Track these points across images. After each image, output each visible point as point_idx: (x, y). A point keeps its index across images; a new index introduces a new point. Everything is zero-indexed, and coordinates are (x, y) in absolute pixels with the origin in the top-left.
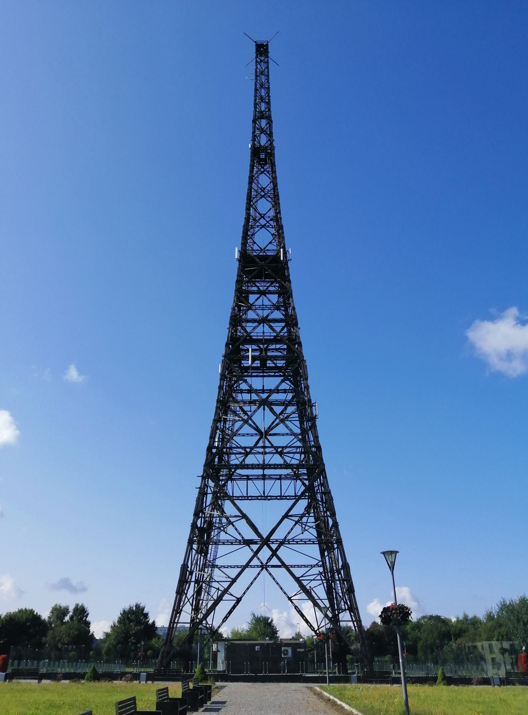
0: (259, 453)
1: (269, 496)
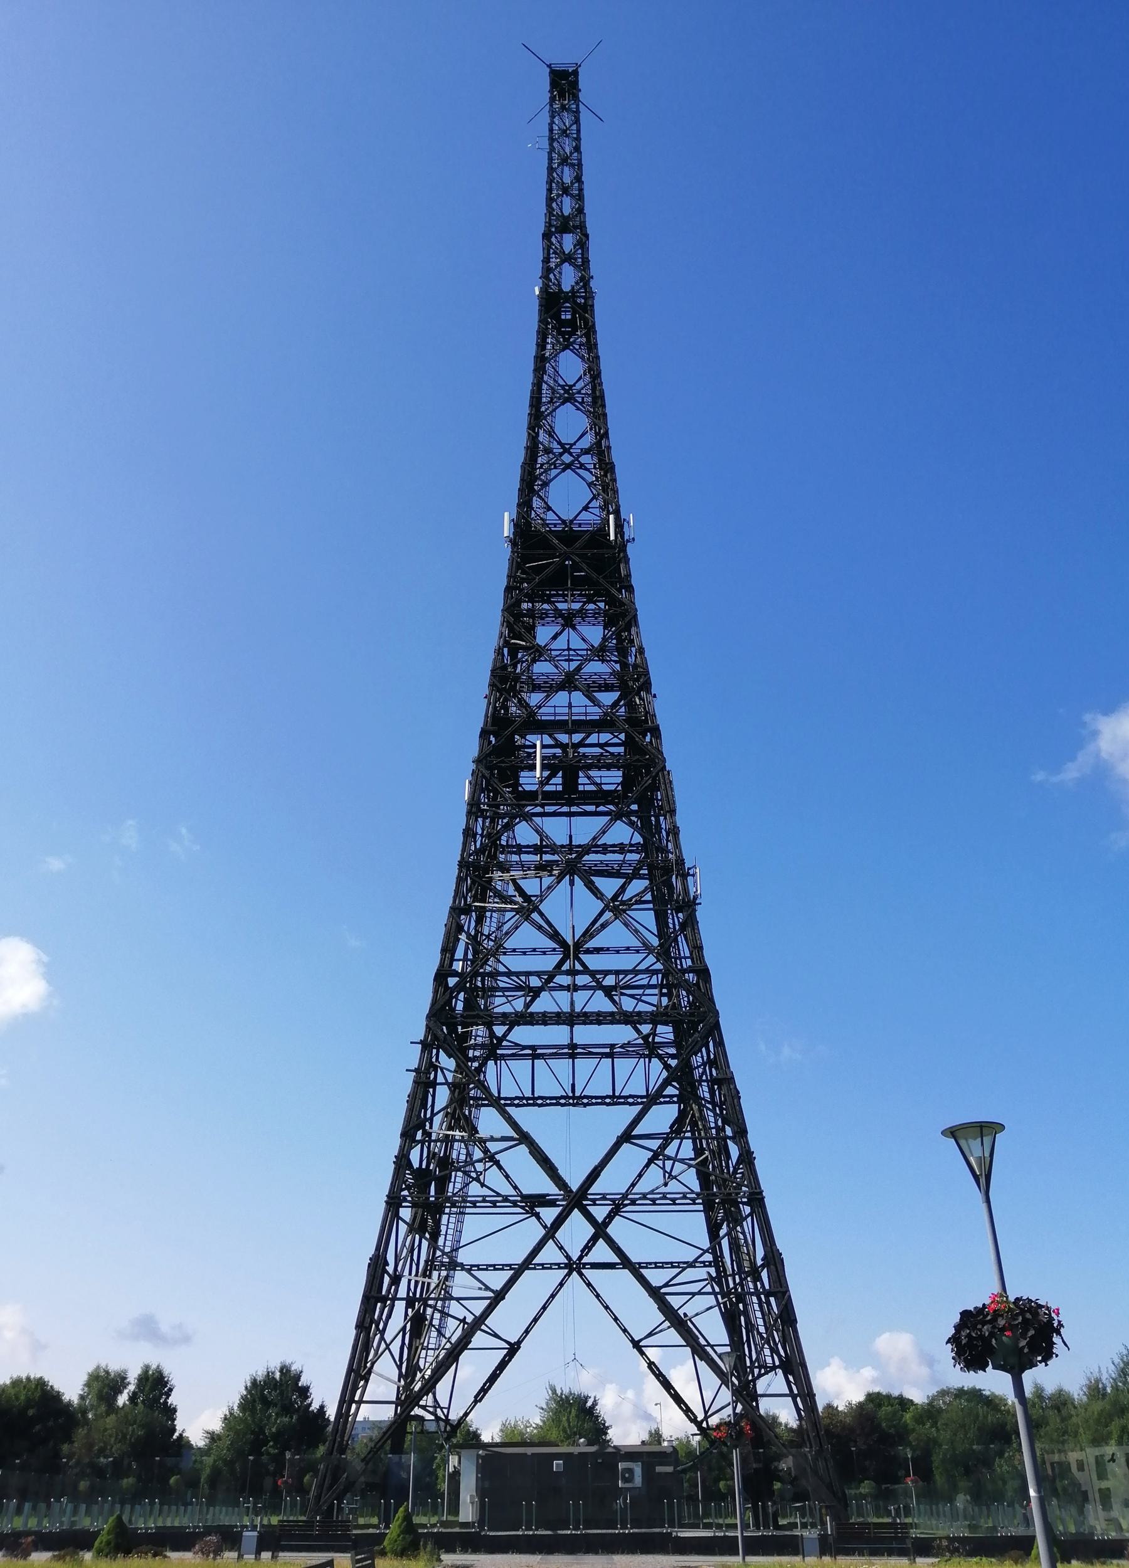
0: (561, 988)
1: (586, 1097)
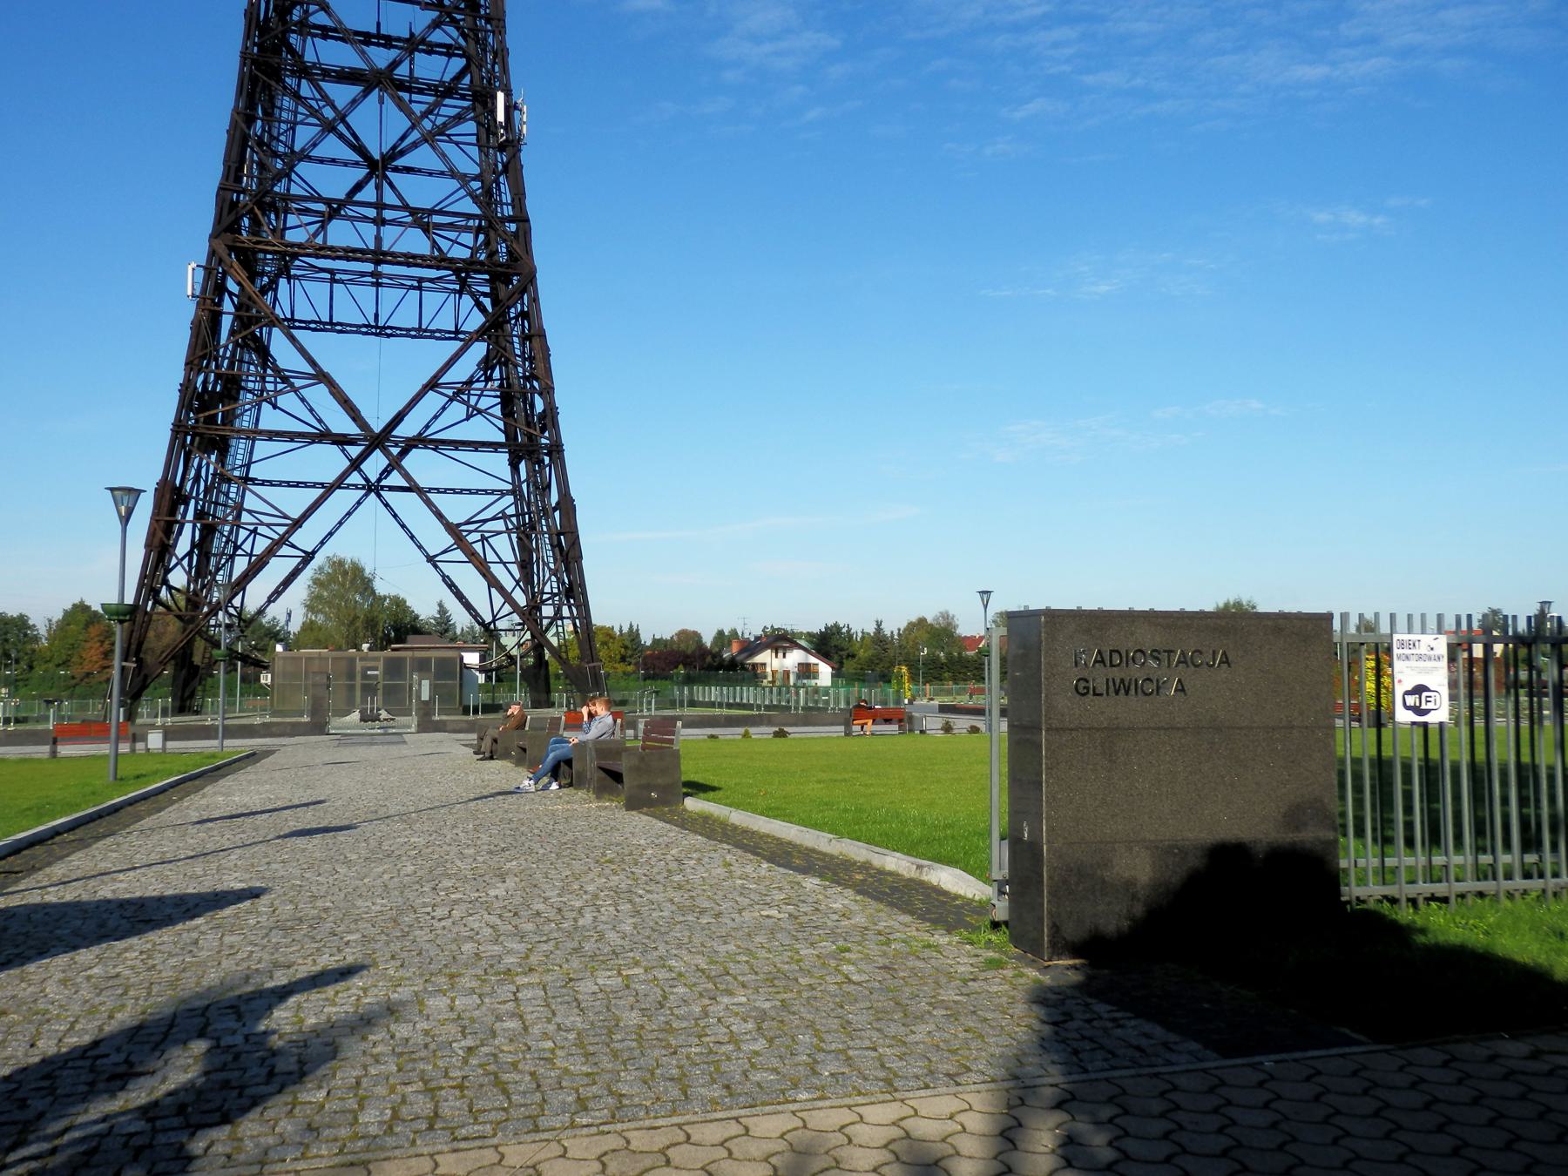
0: (365, 219)
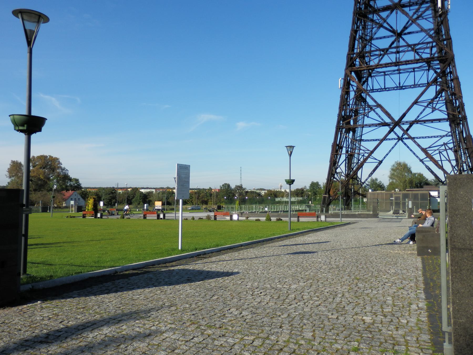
0: (392, 53)
1: (405, 86)
